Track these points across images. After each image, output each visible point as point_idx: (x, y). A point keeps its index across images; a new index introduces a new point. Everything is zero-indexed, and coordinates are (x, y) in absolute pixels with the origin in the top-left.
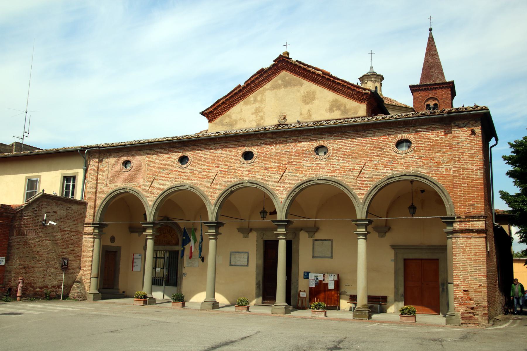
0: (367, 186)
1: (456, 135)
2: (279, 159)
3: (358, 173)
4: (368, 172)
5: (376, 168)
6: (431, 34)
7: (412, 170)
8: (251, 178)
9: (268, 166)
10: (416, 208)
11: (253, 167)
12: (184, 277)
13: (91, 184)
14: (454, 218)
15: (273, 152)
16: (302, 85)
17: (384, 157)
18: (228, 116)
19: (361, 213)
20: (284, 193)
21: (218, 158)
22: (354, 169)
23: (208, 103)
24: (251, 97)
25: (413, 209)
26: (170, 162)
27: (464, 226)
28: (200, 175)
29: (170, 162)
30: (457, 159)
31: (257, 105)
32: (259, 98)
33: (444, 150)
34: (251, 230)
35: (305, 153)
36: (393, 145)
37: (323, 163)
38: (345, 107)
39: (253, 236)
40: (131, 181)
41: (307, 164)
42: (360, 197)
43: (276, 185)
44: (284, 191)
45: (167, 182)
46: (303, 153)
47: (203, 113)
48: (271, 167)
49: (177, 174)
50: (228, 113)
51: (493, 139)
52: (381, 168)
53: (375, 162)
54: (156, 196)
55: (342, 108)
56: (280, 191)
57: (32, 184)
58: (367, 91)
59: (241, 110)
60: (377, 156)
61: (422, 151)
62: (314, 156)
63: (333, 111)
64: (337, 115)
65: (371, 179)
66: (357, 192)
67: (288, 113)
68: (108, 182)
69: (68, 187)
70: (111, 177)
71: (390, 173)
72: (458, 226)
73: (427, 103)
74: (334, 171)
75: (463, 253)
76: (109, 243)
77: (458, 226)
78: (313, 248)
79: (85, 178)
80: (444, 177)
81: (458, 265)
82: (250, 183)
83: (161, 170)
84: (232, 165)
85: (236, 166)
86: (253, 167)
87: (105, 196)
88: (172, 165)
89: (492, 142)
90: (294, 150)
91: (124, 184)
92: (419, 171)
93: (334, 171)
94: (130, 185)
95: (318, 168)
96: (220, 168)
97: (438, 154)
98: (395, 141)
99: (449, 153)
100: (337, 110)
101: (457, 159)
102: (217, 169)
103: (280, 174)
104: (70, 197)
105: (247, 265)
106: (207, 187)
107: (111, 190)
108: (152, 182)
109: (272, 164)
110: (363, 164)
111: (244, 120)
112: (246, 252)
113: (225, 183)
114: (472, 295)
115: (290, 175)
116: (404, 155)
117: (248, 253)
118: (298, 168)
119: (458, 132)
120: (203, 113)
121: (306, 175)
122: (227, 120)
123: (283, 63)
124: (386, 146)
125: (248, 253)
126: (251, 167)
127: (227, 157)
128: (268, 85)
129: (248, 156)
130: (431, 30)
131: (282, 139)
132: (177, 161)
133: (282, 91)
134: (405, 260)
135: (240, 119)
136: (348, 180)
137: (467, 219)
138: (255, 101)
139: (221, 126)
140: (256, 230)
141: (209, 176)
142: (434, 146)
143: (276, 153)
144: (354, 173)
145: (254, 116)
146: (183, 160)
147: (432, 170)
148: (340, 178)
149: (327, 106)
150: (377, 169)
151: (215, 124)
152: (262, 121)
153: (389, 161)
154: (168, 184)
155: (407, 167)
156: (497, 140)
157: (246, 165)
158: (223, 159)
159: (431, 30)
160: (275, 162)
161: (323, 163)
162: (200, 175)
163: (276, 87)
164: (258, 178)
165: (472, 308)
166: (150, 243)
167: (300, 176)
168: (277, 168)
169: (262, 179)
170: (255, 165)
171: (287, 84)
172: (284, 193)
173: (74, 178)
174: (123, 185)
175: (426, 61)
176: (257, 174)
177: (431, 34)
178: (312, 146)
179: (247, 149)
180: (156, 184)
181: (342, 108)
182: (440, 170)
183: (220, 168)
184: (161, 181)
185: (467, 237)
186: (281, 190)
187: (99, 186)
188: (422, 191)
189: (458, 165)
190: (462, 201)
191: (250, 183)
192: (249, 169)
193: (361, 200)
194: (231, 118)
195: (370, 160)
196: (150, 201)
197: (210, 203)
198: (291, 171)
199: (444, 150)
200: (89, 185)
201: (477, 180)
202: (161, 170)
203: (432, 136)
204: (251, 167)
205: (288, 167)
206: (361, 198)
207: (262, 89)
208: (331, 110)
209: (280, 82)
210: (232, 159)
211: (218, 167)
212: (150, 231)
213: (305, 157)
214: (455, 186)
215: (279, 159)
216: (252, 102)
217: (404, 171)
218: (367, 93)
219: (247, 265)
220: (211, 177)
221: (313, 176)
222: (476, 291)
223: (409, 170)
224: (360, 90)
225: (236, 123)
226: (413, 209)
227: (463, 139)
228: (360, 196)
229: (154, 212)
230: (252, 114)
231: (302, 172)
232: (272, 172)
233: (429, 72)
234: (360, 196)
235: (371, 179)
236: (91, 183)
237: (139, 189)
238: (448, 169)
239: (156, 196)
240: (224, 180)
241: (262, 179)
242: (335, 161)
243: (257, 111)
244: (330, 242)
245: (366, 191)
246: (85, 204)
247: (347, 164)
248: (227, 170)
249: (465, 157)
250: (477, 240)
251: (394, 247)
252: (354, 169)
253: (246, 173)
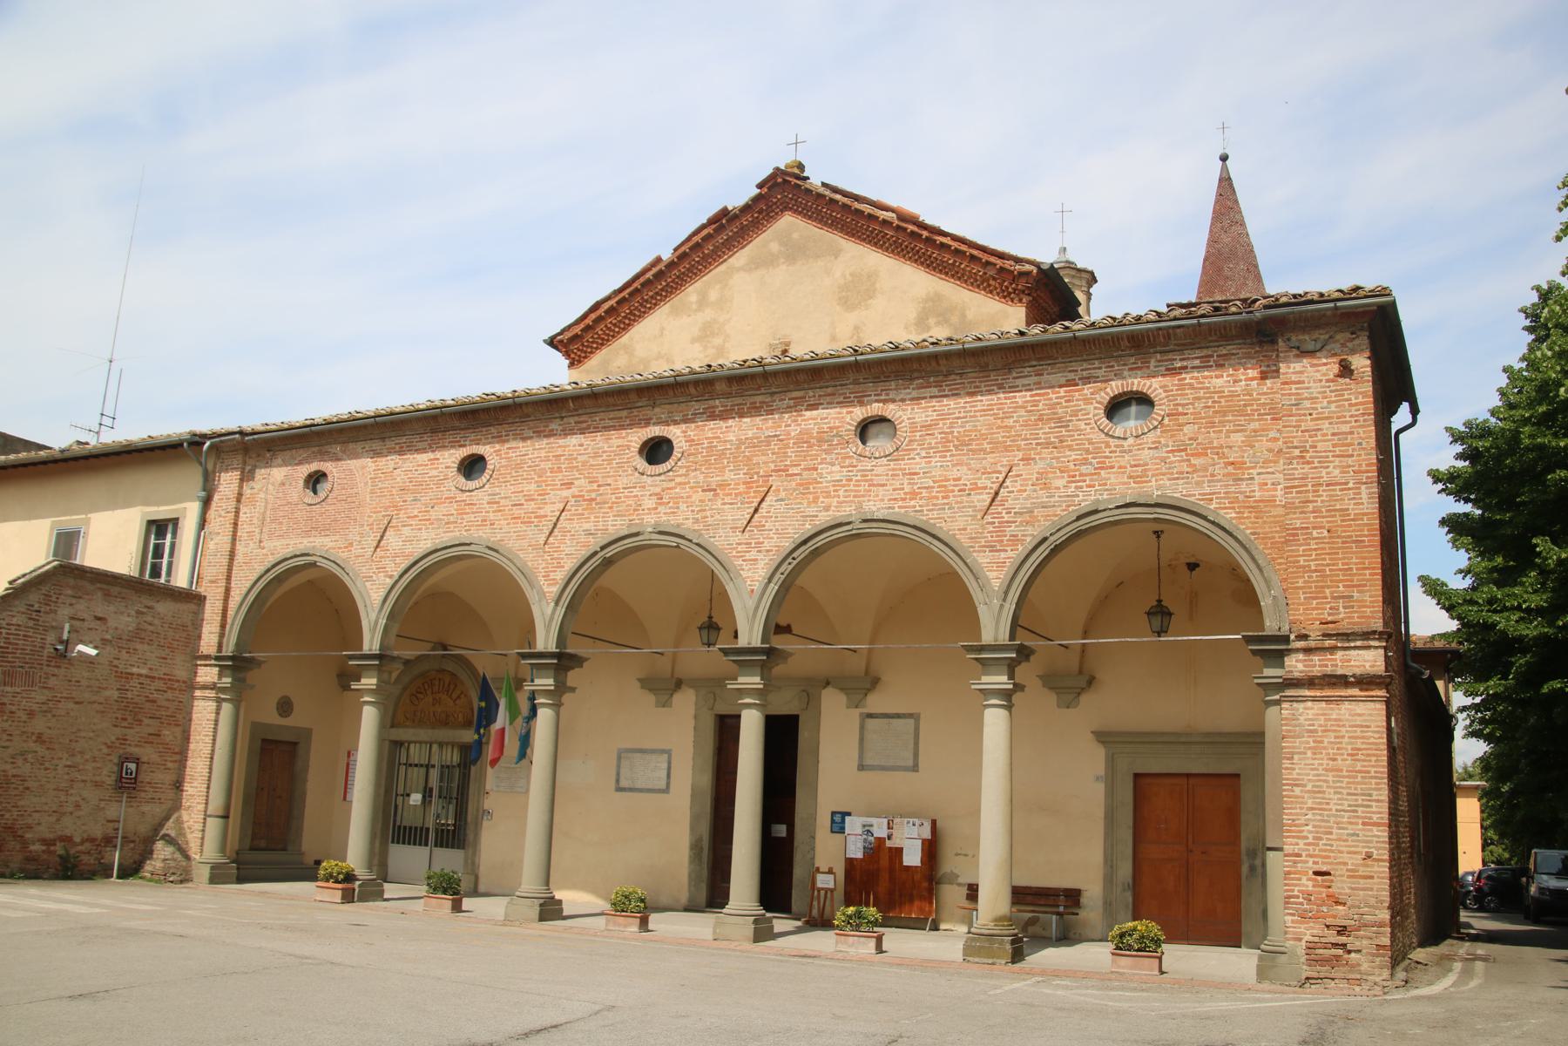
0: (1015, 540)
2: (749, 458)
4: (1017, 497)
5: (1043, 482)
6: (1225, 169)
7: (1155, 489)
9: (715, 480)
10: (1170, 614)
11: (672, 484)
12: (485, 823)
13: (218, 542)
14: (1286, 639)
15: (731, 437)
16: (836, 253)
17: (1070, 448)
19: (994, 627)
20: (761, 564)
21: (571, 459)
22: (975, 487)
23: (568, 310)
24: (691, 293)
25: (1160, 615)
26: (435, 473)
27: (1318, 665)
28: (517, 511)
30: (1297, 452)
31: (708, 314)
32: (713, 295)
34: (679, 684)
36: (1096, 411)
37: (881, 468)
38: (963, 316)
39: (685, 702)
40: (324, 530)
41: (831, 473)
42: (991, 575)
43: (737, 537)
44: (761, 556)
46: (821, 441)
47: (552, 342)
48: (722, 485)
50: (625, 339)
51: (1405, 407)
52: (1060, 483)
55: (955, 319)
57: (67, 541)
58: (1028, 267)
59: (662, 329)
60: (1048, 444)
61: (1186, 429)
66: (983, 559)
69: (158, 552)
70: (273, 521)
71: (1085, 501)
72: (1300, 666)
76: (272, 718)
77: (1300, 666)
78: (862, 740)
79: (203, 523)
80: (1257, 508)
81: (1297, 790)
83: (409, 498)
84: (609, 481)
85: (623, 481)
86: (672, 484)
87: (256, 576)
88: (438, 484)
89: (1402, 416)
90: (794, 431)
91: (305, 541)
92: (1178, 491)
94: (322, 545)
95: (864, 487)
96: (574, 490)
97: (1238, 438)
98: (1104, 397)
99: (1272, 434)
101: (1297, 452)
102: (566, 493)
103: (749, 506)
104: (162, 580)
105: (667, 790)
106: (535, 547)
108: (381, 532)
109: (729, 475)
112: (663, 751)
114: (1341, 886)
115: (781, 506)
116: (1131, 441)
117: (668, 752)
118: (805, 485)
120: (552, 342)
121: (827, 509)
123: (785, 192)
125: (668, 752)
126: (665, 485)
127: (596, 455)
128: (740, 258)
129: (656, 451)
130: (1224, 158)
131: (759, 399)
134: (1137, 776)
136: (957, 522)
137: (1328, 643)
138: (703, 303)
140: (696, 683)
141: (542, 512)
142: (1224, 414)
143: (741, 442)
144: (975, 498)
145: (697, 347)
146: (472, 466)
147: (1218, 487)
148: (929, 516)
150: (1046, 486)
153: (1085, 462)
154: (426, 540)
156: (1415, 411)
158: (584, 463)
159: (1224, 158)
160: (737, 469)
161: (879, 470)
162: (517, 511)
164: (683, 518)
165: (1342, 930)
166: (369, 717)
167: (812, 510)
168: (742, 488)
169: (696, 521)
170: (678, 480)
171: (794, 252)
172: (761, 564)
174: (303, 544)
175: (1213, 241)
176: (683, 507)
177: (1225, 169)
179: (655, 431)
182: (1244, 486)
183: (574, 490)
184: (406, 531)
186: (753, 554)
187: (240, 548)
188: (1192, 566)
189: (1300, 470)
190: (1312, 585)
192: (658, 490)
195: (1027, 460)
196: (373, 593)
197: (542, 594)
198: (783, 495)
200: (211, 545)
202: (409, 498)
203: (1219, 382)
205: (775, 481)
209: (774, 247)
210: (610, 461)
211: (569, 485)
212: (369, 682)
213: (827, 452)
214: (1292, 536)
215: (749, 458)
217: (1131, 492)
218: (1028, 273)
219: (667, 790)
220: (546, 517)
221: (847, 511)
222: (1353, 874)
224: (1008, 264)
226: (1160, 615)
227: (1315, 389)
228: (993, 574)
229: (382, 622)
230: (694, 341)
233: (1220, 269)
234: (993, 574)
236: (217, 539)
238: (1268, 482)
240: (586, 526)
241: (696, 521)
242: (918, 464)
244: (912, 721)
245: (1012, 555)
246: (200, 600)
247: (955, 473)
250: (1360, 708)
251: (1103, 737)
252: (975, 487)
253: (649, 503)
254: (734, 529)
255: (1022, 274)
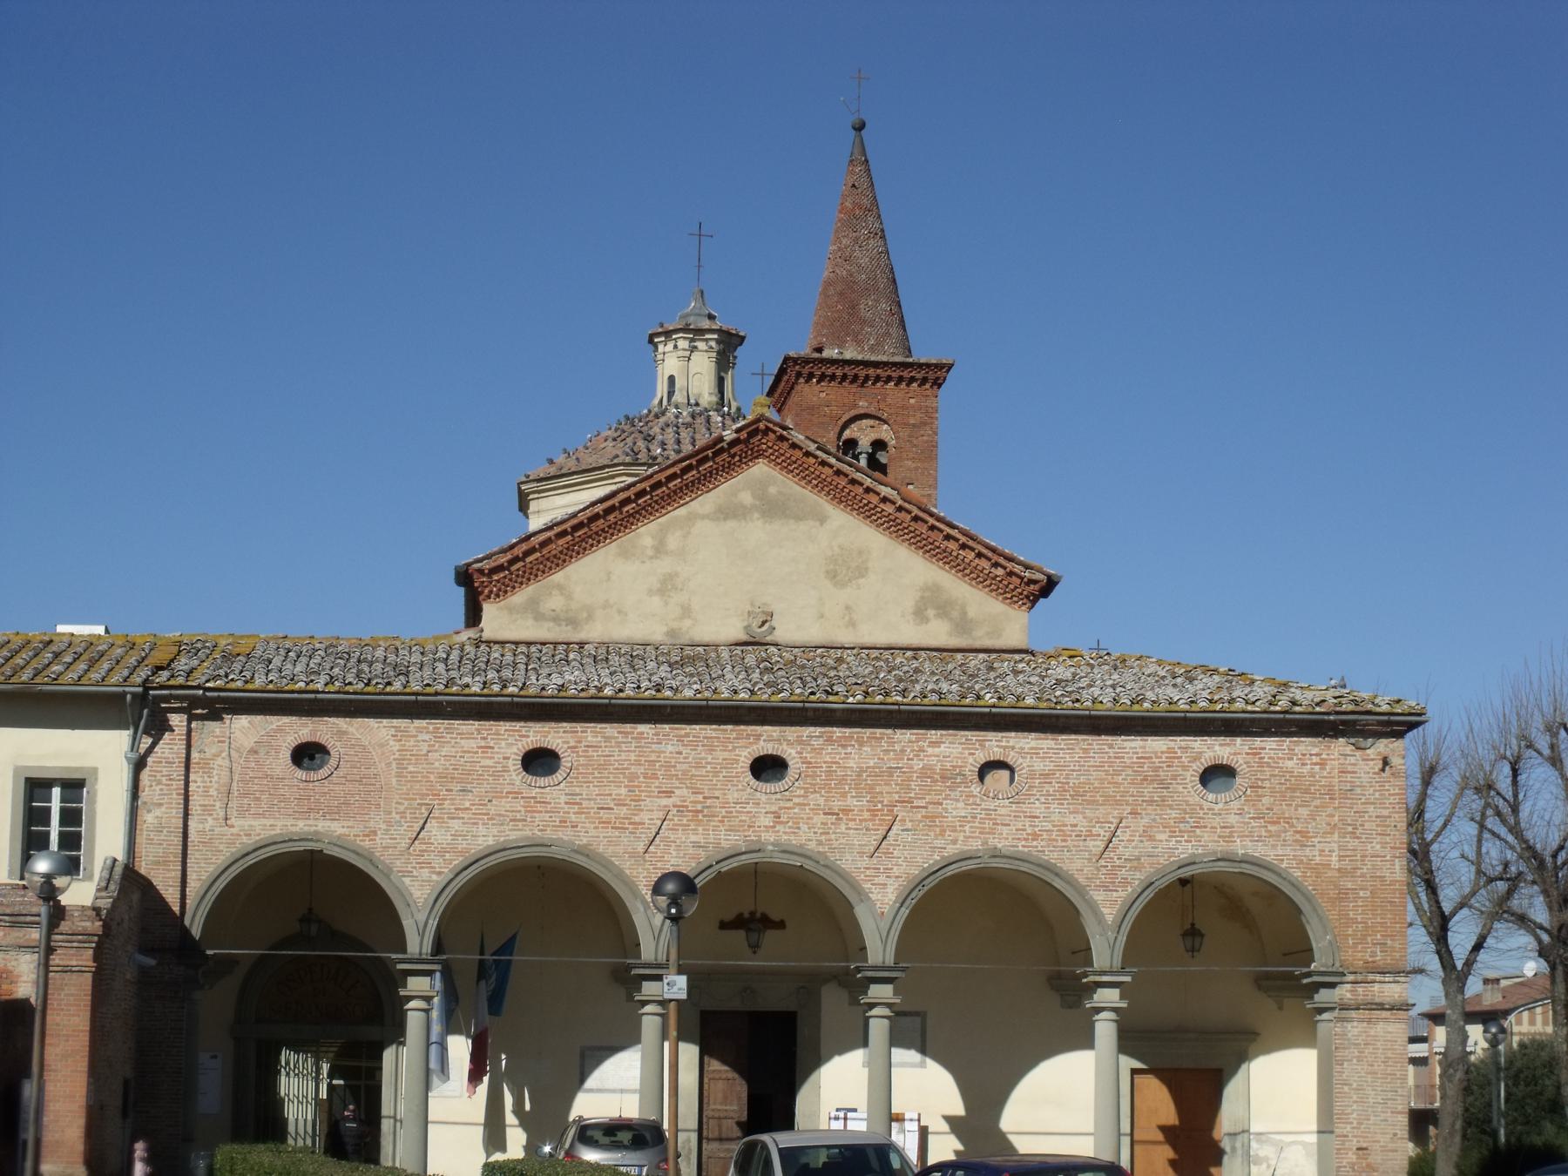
0: (1125, 882)
1: (1350, 768)
2: (872, 787)
3: (1102, 845)
4: (1127, 845)
5: (1147, 835)
7: (1240, 847)
8: (784, 835)
9: (837, 804)
11: (789, 804)
13: (160, 815)
15: (852, 764)
16: (822, 520)
17: (1171, 807)
18: (560, 587)
20: (890, 889)
21: (668, 766)
24: (645, 534)
26: (489, 762)
29: (489, 762)
30: (1350, 829)
31: (664, 565)
32: (673, 541)
33: (1317, 802)
35: (949, 777)
37: (1004, 808)
38: (964, 613)
40: (332, 813)
41: (955, 809)
42: (1105, 911)
43: (866, 862)
44: (891, 881)
45: (482, 830)
48: (846, 811)
49: (519, 805)
50: (558, 577)
53: (1145, 821)
54: (439, 873)
55: (955, 614)
56: (876, 880)
59: (609, 574)
60: (1150, 802)
61: (1265, 800)
62: (976, 789)
63: (927, 620)
64: (938, 633)
65: (1135, 863)
66: (1098, 896)
67: (776, 607)
68: (233, 813)
72: (1349, 995)
73: (847, 434)
74: (1035, 836)
75: (1359, 1059)
77: (1349, 995)
80: (1319, 870)
81: (1346, 1089)
82: (784, 852)
83: (456, 787)
84: (717, 794)
85: (733, 796)
86: (789, 804)
88: (496, 775)
91: (301, 824)
92: (1259, 851)
93: (1035, 836)
97: (1304, 812)
98: (1199, 767)
99: (1329, 811)
100: (938, 616)
101: (1350, 829)
102: (665, 802)
106: (633, 855)
107: (245, 839)
109: (851, 802)
110: (1115, 821)
111: (620, 612)
113: (696, 845)
114: (1375, 1158)
116: (1221, 806)
118: (932, 818)
119: (1352, 760)
121: (955, 842)
122: (555, 603)
124: (1174, 778)
126: (782, 804)
128: (705, 503)
129: (768, 767)
130: (860, 127)
132: (515, 764)
133: (756, 531)
135: (606, 605)
138: (660, 550)
139: (530, 622)
141: (637, 819)
142: (1294, 790)
143: (862, 771)
145: (656, 600)
147: (1288, 850)
148: (1051, 856)
149: (909, 604)
150: (1151, 838)
151: (511, 610)
152: (687, 623)
153: (1183, 820)
155: (1228, 838)
157: (764, 798)
158: (685, 773)
161: (1002, 811)
163: (728, 512)
167: (939, 843)
168: (866, 815)
169: (820, 843)
170: (796, 800)
171: (772, 509)
172: (890, 889)
173: (74, 786)
174: (301, 826)
176: (804, 827)
178: (971, 760)
180: (436, 833)
181: (955, 614)
182: (1308, 851)
184: (456, 825)
185: (1369, 1021)
186: (882, 879)
189: (1355, 843)
191: (784, 852)
192: (774, 808)
193: (1109, 919)
194: (569, 597)
195: (1134, 813)
198: (909, 825)
199: (1317, 802)
201: (1393, 882)
202: (456, 787)
203: (1290, 764)
204: (782, 804)
206: (1109, 914)
207: (682, 511)
208: (920, 614)
209: (746, 498)
210: (716, 774)
211: (669, 794)
213: (951, 789)
214: (1343, 896)
215: (872, 787)
216: (650, 552)
217: (1221, 847)
221: (975, 845)
222: (1384, 1150)
223: (1232, 847)
225: (590, 617)
227: (1365, 779)
228: (1107, 907)
229: (433, 924)
230: (650, 592)
231: (943, 832)
232: (851, 824)
233: (854, 306)
234: (1107, 907)
235: (1135, 863)
237: (367, 844)
238: (1327, 851)
239: (439, 873)
240: (693, 838)
241: (820, 843)
242: (1038, 808)
243: (666, 586)
244: (918, 1020)
245: (1122, 895)
247: (1071, 819)
248: (699, 807)
249: (1367, 826)
250: (1392, 1027)
253: (767, 821)
254: (861, 853)
255: (1031, 582)
